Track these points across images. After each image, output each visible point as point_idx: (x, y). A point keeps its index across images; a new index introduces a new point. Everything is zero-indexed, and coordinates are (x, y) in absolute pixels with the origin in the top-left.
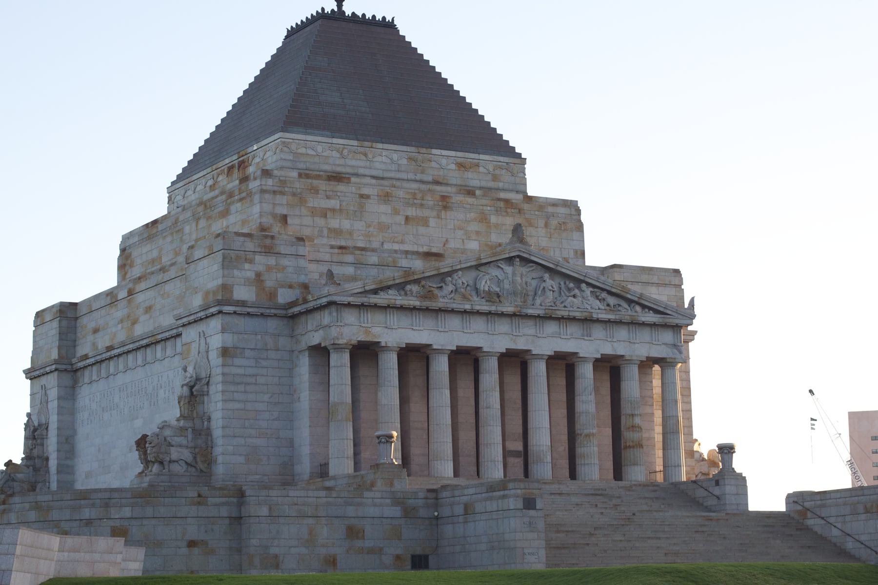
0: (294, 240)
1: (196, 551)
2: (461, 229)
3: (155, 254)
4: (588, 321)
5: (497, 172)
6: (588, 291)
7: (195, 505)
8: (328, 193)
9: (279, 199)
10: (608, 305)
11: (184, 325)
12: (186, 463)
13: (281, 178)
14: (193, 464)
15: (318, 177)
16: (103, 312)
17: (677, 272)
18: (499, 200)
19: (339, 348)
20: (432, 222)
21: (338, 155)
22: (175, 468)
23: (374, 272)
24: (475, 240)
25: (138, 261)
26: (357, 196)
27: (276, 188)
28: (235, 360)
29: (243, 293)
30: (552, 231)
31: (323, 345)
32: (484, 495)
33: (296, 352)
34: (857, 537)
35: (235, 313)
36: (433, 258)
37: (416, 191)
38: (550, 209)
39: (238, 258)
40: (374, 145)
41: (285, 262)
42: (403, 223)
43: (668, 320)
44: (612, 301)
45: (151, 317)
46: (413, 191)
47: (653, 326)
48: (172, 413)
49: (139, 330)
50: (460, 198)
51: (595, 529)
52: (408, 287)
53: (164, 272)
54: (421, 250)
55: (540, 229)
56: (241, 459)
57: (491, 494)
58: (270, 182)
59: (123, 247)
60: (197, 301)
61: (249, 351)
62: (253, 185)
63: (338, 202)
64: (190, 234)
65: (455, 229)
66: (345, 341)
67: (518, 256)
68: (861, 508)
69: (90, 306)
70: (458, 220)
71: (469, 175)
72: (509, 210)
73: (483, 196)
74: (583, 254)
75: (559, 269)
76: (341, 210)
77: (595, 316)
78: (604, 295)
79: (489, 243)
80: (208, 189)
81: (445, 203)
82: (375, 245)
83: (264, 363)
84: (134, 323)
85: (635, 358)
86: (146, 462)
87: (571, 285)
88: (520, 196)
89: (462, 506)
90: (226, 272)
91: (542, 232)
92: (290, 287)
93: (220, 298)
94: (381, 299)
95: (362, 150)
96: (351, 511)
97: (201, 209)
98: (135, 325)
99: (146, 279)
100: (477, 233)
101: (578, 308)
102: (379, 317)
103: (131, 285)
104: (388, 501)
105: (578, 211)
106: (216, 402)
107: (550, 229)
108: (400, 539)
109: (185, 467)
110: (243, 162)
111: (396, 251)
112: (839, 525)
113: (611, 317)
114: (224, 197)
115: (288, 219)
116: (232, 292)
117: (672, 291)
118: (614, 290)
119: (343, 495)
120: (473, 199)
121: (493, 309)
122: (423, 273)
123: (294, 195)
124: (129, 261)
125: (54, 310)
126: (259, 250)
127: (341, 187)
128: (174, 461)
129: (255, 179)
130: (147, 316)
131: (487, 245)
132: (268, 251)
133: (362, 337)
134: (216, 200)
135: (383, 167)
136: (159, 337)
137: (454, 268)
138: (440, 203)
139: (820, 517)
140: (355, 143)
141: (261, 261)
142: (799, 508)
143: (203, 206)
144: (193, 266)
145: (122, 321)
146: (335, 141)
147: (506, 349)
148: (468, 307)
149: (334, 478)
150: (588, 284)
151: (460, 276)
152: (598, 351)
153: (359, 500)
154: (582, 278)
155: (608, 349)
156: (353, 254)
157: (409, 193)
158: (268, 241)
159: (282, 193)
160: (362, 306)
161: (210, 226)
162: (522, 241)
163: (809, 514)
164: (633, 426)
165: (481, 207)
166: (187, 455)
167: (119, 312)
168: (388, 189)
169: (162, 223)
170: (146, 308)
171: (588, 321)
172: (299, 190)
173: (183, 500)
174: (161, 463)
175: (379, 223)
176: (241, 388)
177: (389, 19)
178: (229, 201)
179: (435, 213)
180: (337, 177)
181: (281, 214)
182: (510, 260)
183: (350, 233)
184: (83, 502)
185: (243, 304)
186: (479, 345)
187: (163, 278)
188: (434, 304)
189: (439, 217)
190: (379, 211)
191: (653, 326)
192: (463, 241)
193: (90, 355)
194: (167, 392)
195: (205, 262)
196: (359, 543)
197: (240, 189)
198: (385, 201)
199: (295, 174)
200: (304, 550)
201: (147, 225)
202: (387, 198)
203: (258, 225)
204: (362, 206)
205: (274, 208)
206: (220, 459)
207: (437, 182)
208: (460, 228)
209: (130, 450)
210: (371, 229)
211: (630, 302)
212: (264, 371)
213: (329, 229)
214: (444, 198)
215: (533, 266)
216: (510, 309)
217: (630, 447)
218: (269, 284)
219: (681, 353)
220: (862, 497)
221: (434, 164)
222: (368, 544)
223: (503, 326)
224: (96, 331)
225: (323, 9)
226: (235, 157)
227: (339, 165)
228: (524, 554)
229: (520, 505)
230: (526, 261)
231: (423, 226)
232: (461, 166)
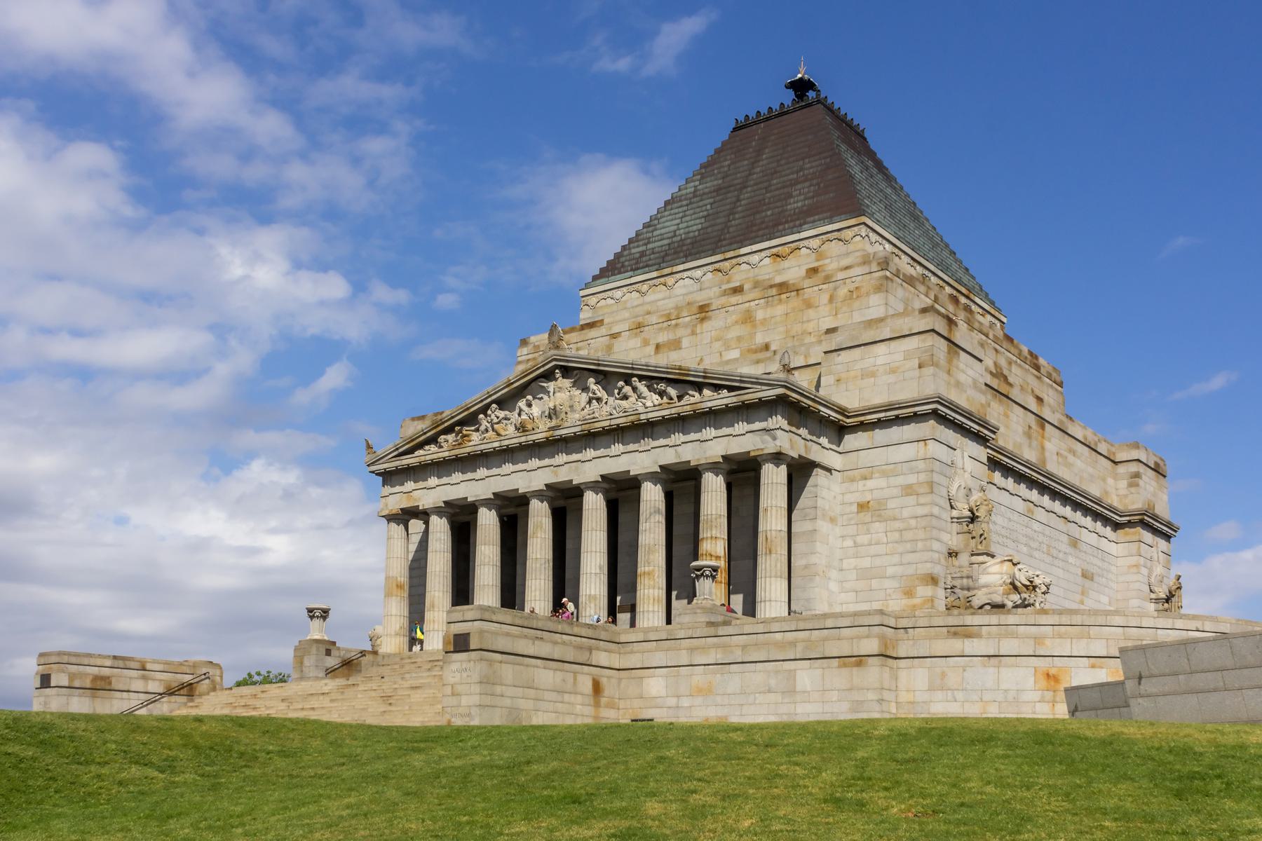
2: (719, 340)
6: (642, 387)
13: (536, 344)
18: (771, 286)
24: (735, 348)
30: (839, 305)
37: (672, 311)
40: (676, 269)
42: (653, 353)
43: (746, 397)
44: (672, 392)
46: (668, 312)
50: (724, 300)
55: (820, 308)
58: (525, 350)
63: (587, 351)
65: (711, 342)
70: (716, 330)
72: (784, 296)
73: (755, 288)
78: (662, 386)
79: (753, 347)
81: (704, 311)
91: (824, 310)
95: (662, 280)
100: (739, 339)
101: (625, 412)
107: (836, 303)
120: (737, 298)
122: (453, 417)
135: (684, 291)
137: (485, 402)
140: (655, 274)
152: (657, 463)
157: (662, 316)
165: (747, 304)
168: (640, 319)
179: (689, 331)
182: (548, 376)
189: (693, 333)
192: (721, 355)
202: (639, 330)
208: (718, 340)
211: (699, 387)
215: (577, 375)
216: (539, 436)
231: (675, 350)
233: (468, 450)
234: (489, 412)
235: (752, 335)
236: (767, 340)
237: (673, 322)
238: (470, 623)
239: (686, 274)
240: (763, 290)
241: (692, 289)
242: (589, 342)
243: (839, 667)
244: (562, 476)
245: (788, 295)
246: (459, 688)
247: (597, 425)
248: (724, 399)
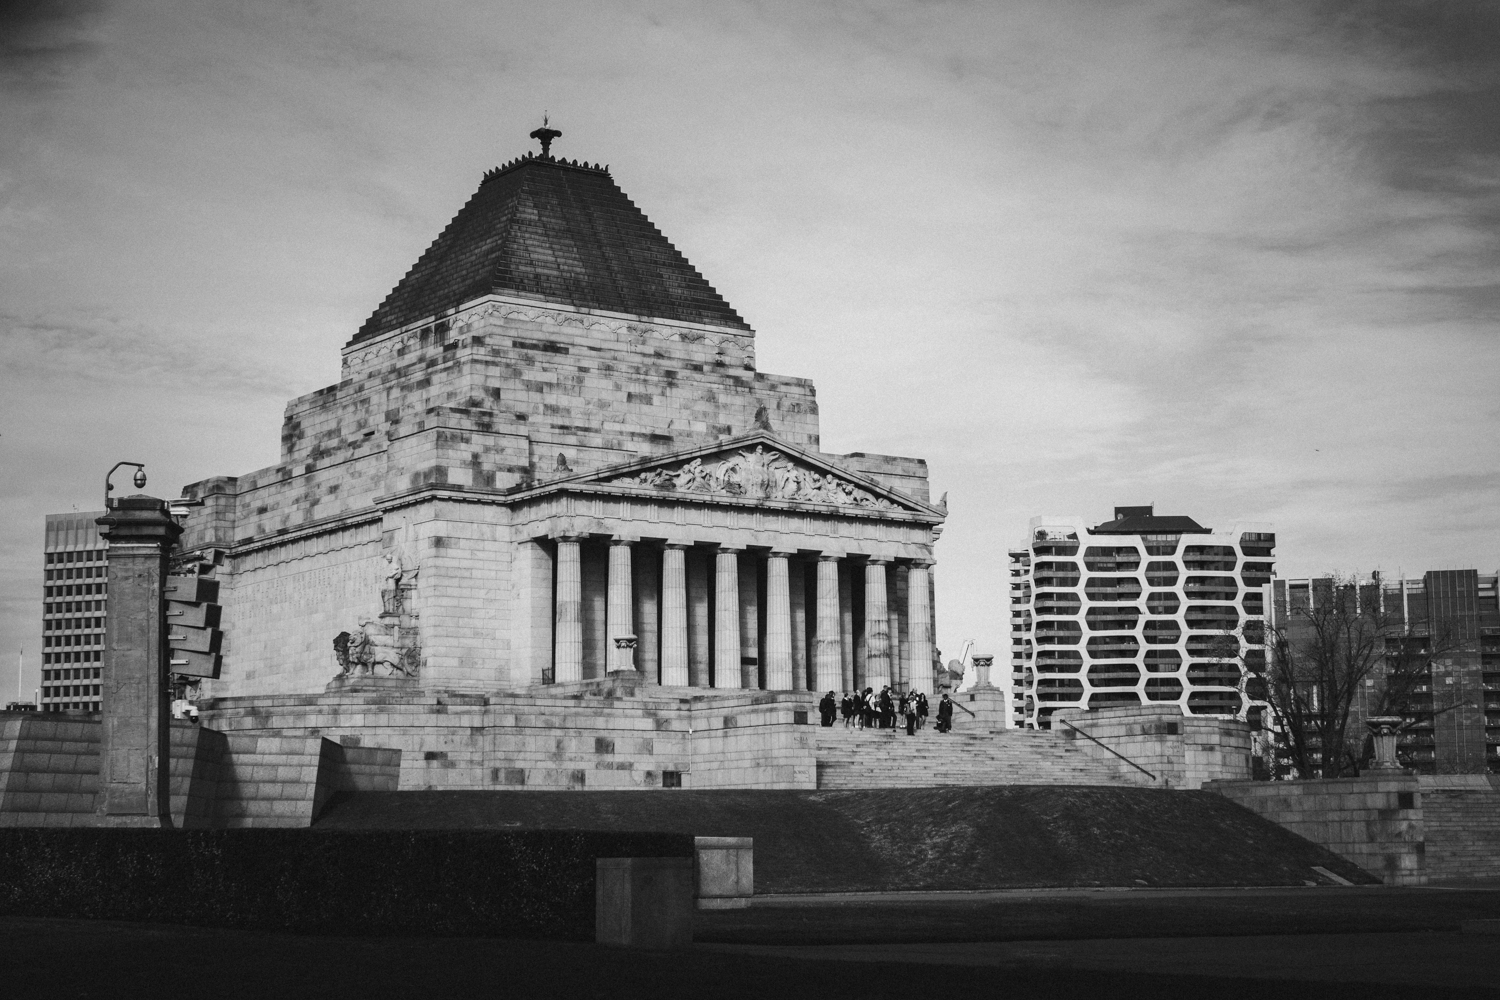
0: (514, 418)
1: (435, 763)
3: (333, 425)
4: (834, 516)
5: (724, 345)
7: (430, 713)
8: (546, 365)
9: (495, 371)
10: (855, 499)
11: (386, 511)
12: (392, 664)
14: (400, 666)
15: (534, 347)
16: (273, 489)
17: (922, 462)
18: (729, 377)
19: (566, 539)
20: (656, 400)
21: (553, 321)
22: (379, 669)
23: (597, 455)
25: (309, 432)
26: (576, 369)
27: (489, 358)
28: (449, 551)
31: (550, 537)
32: (747, 708)
33: (516, 544)
34: (1132, 761)
35: (450, 499)
36: (661, 442)
37: (640, 366)
38: (783, 389)
39: (453, 437)
40: (593, 311)
41: (504, 442)
42: (625, 400)
43: (917, 517)
44: (859, 494)
45: (336, 498)
49: (319, 513)
50: (687, 373)
51: (858, 746)
52: (643, 475)
53: (354, 448)
54: (644, 431)
56: (455, 662)
57: (756, 707)
58: (482, 350)
59: (288, 415)
60: (403, 485)
61: (464, 541)
62: (463, 354)
63: (555, 375)
64: (379, 405)
66: (576, 534)
67: (762, 443)
68: (1137, 729)
69: (255, 482)
71: (694, 347)
72: (739, 389)
73: (713, 372)
74: (817, 440)
75: (804, 458)
76: (558, 384)
77: (841, 511)
78: (850, 487)
80: (395, 353)
82: (594, 424)
83: (480, 555)
84: (315, 503)
85: (882, 558)
86: (347, 664)
87: (817, 476)
88: (751, 374)
89: (722, 719)
90: (440, 451)
92: (510, 470)
93: (433, 480)
94: (617, 487)
96: (600, 722)
97: (393, 376)
98: (316, 507)
99: (331, 455)
100: (705, 414)
103: (310, 461)
104: (640, 712)
105: (813, 392)
106: (426, 598)
108: (651, 753)
109: (390, 669)
110: (442, 324)
111: (621, 433)
112: (1112, 747)
113: (859, 512)
114: (424, 365)
115: (501, 393)
116: (446, 475)
117: (915, 484)
118: (862, 483)
119: (591, 705)
121: (734, 501)
123: (508, 366)
124: (297, 432)
125: (210, 485)
126: (476, 428)
127: (559, 358)
128: (379, 663)
129: (465, 347)
130: (332, 497)
131: (714, 427)
132: (486, 428)
133: (595, 530)
134: (412, 368)
135: (600, 336)
136: (349, 521)
138: (665, 379)
139: (1089, 738)
140: (572, 308)
141: (479, 441)
142: (1067, 728)
143: (396, 373)
144: (397, 444)
145: (297, 501)
146: (550, 305)
147: (748, 546)
148: (707, 498)
149: (561, 685)
150: (835, 476)
151: (699, 463)
153: (606, 711)
154: (828, 468)
155: (854, 548)
156: (575, 434)
158: (486, 419)
159: (494, 364)
161: (405, 397)
162: (766, 426)
163: (1078, 735)
164: (879, 634)
165: (709, 385)
166: (393, 656)
167: (298, 489)
169: (341, 390)
170: (331, 488)
171: (834, 516)
172: (513, 361)
173: (421, 707)
174: (365, 664)
175: (599, 400)
176: (455, 582)
177: (602, 166)
178: (430, 370)
179: (659, 390)
180: (552, 347)
181: (493, 388)
182: (751, 448)
183: (568, 411)
184: (308, 708)
185: (459, 488)
186: (718, 541)
187: (353, 454)
188: (671, 494)
189: (663, 394)
193: (256, 538)
194: (357, 584)
195: (413, 440)
196: (608, 758)
197: (444, 357)
198: (606, 375)
199: (509, 343)
200: (551, 765)
201: (321, 392)
203: (468, 398)
204: (580, 380)
205: (486, 380)
206: (430, 662)
207: (658, 355)
208: (686, 408)
209: (308, 648)
210: (591, 406)
211: (878, 496)
212: (479, 564)
213: (545, 406)
214: (670, 374)
216: (752, 497)
217: (875, 656)
218: (487, 467)
219: (930, 553)
220: (1139, 717)
221: (655, 334)
222: (617, 758)
223: (745, 520)
224: (262, 510)
225: (530, 154)
226: (433, 318)
227: (553, 333)
228: (795, 772)
229: (791, 719)
230: (768, 448)
232: (684, 337)
233: (678, 495)
234: (693, 464)
235: (716, 415)
236: (729, 423)
237: (642, 377)
238: (1174, 717)
239: (602, 320)
240: (722, 376)
241: (608, 337)
242: (556, 366)
243: (1203, 750)
245: (743, 389)
246: (1174, 759)
247: (802, 506)
248: (906, 515)
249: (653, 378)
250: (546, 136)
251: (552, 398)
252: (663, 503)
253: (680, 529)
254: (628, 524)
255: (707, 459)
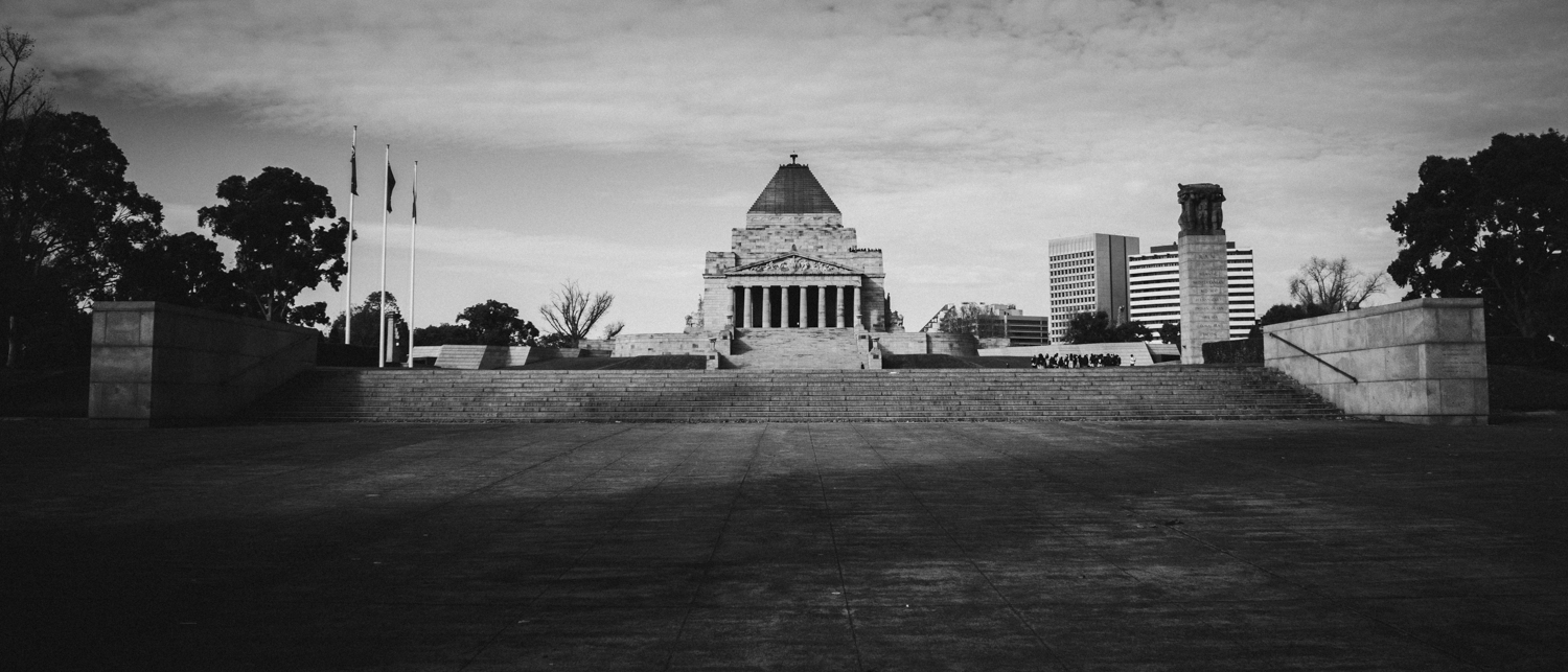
4: (821, 275)
17: (880, 251)
29: (713, 271)
47: (848, 275)
48: (696, 309)
81: (801, 233)
94: (743, 272)
102: (746, 278)
127: (761, 231)
141: (719, 261)
160: (736, 275)
162: (795, 250)
171: (821, 275)
182: (791, 257)
190: (774, 238)
191: (848, 275)
216: (789, 273)
223: (789, 278)
230: (796, 257)
244: (795, 284)
248: (849, 272)
249: (795, 233)
250: (794, 157)
251: (758, 244)
252: (759, 275)
253: (766, 283)
254: (747, 283)
255: (774, 262)
